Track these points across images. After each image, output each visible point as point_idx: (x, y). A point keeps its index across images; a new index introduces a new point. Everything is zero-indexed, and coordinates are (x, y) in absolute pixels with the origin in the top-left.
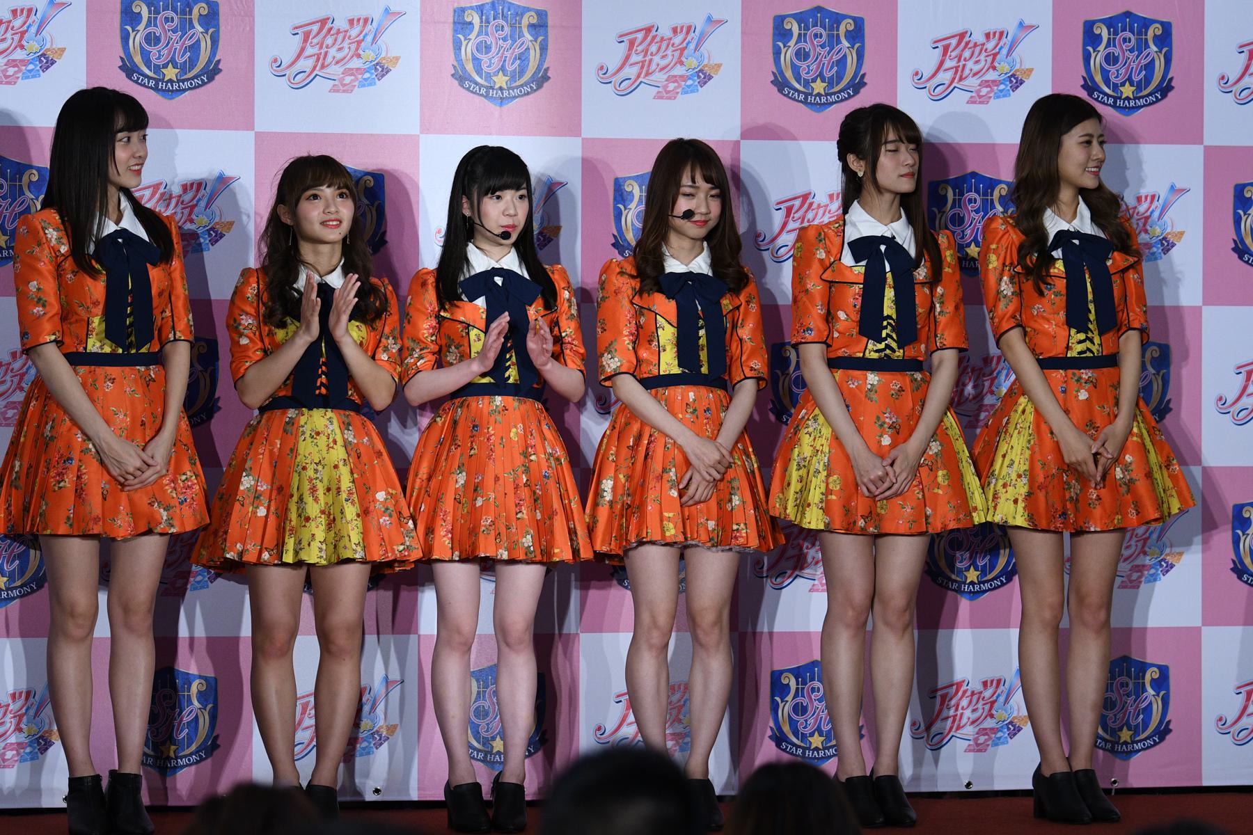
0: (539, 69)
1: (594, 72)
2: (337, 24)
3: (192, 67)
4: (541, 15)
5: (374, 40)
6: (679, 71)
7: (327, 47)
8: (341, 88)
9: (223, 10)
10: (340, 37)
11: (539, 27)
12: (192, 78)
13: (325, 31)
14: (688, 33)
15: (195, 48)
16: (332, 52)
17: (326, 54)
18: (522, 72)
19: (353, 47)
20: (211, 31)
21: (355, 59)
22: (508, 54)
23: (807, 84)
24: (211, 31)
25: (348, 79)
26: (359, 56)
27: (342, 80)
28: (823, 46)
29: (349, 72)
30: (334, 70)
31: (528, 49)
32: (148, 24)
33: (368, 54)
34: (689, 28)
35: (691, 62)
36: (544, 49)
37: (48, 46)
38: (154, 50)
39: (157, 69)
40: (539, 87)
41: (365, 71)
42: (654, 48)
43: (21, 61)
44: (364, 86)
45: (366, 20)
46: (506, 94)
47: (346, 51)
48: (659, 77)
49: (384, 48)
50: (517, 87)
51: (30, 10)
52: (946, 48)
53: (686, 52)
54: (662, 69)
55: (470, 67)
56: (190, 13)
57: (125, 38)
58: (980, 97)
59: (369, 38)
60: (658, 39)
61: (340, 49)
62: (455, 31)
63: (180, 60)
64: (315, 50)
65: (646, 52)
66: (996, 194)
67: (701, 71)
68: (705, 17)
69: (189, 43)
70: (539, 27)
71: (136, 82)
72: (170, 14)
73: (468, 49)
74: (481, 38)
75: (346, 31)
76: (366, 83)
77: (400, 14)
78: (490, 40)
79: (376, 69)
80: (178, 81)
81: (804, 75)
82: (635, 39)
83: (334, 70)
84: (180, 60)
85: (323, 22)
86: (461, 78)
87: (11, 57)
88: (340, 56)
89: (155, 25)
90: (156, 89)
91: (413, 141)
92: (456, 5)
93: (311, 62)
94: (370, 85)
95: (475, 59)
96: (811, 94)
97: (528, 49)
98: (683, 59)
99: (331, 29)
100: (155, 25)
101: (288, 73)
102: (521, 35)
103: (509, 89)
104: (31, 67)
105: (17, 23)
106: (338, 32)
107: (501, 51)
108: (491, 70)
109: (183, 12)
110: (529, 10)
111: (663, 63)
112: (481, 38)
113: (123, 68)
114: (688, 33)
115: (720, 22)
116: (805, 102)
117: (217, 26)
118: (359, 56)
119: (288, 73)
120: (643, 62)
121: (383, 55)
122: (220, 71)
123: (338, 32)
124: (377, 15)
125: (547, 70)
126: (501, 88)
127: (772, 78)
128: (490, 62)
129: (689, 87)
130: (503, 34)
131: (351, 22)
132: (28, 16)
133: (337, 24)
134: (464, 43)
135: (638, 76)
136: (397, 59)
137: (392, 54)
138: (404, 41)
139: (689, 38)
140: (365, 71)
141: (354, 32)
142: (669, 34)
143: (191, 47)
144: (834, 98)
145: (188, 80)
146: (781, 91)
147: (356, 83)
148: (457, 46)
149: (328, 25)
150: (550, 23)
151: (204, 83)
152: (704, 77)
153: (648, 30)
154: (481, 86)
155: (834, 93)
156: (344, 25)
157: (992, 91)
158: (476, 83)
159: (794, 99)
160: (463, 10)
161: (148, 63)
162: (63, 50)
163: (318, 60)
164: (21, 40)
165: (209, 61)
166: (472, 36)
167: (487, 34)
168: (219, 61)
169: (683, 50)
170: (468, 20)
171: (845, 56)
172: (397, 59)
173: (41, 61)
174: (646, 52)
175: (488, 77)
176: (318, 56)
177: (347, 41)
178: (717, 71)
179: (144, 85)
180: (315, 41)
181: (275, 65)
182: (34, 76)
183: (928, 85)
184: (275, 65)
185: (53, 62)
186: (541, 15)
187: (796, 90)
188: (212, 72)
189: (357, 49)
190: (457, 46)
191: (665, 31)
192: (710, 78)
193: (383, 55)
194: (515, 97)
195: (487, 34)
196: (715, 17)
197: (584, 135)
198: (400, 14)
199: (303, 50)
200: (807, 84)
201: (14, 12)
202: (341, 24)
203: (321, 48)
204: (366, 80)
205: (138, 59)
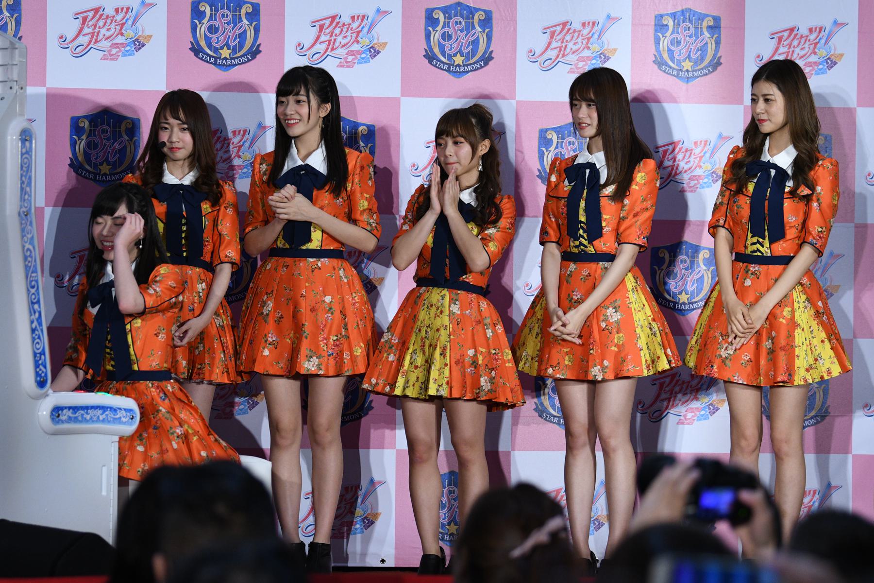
0: (714, 56)
2: (574, 26)
3: (473, 55)
4: (717, 19)
6: (813, 58)
7: (567, 42)
9: (494, 16)
12: (474, 63)
13: (565, 31)
14: (820, 32)
15: (475, 43)
16: (570, 45)
17: (566, 46)
18: (702, 59)
19: (585, 42)
20: (487, 30)
22: (692, 47)
24: (487, 30)
26: (588, 48)
27: (576, 65)
30: (572, 58)
31: (707, 43)
32: (444, 26)
33: (595, 47)
34: (821, 28)
35: (822, 52)
36: (718, 43)
37: (375, 41)
38: (447, 44)
39: (450, 57)
40: (715, 69)
41: (594, 58)
42: (795, 43)
43: (357, 51)
45: (594, 23)
46: (691, 75)
47: (580, 44)
49: (606, 43)
51: (363, 17)
52: (85, 20)
53: (818, 46)
55: (666, 56)
56: (473, 18)
59: (596, 36)
60: (798, 36)
61: (575, 43)
62: (656, 31)
63: (465, 51)
64: (559, 44)
65: (790, 45)
67: (829, 59)
68: (832, 21)
69: (472, 39)
70: (715, 28)
71: (435, 66)
72: (459, 19)
73: (665, 43)
77: (617, 19)
78: (680, 37)
79: (600, 58)
80: (464, 66)
82: (782, 36)
83: (572, 58)
84: (465, 51)
85: (564, 24)
86: (660, 63)
87: (350, 49)
88: (575, 48)
89: (449, 27)
90: (448, 71)
92: (657, 13)
93: (556, 52)
95: (669, 50)
97: (707, 43)
98: (816, 50)
99: (569, 29)
101: (539, 60)
102: (702, 34)
104: (364, 55)
105: (355, 25)
106: (575, 31)
107: (688, 44)
108: (681, 58)
110: (707, 16)
114: (820, 32)
115: (843, 25)
117: (491, 27)
118: (588, 48)
119: (539, 60)
121: (605, 47)
122: (493, 58)
123: (575, 31)
124: (601, 20)
126: (687, 71)
128: (680, 52)
129: (820, 70)
130: (690, 33)
131: (584, 24)
132: (362, 21)
133: (574, 26)
134: (662, 39)
136: (615, 50)
139: (821, 36)
140: (594, 58)
141: (585, 32)
143: (473, 42)
148: (657, 41)
149: (568, 27)
150: (722, 25)
151: (481, 67)
153: (792, 30)
154: (673, 69)
158: (671, 68)
160: (661, 16)
161: (443, 53)
163: (560, 50)
165: (485, 52)
166: (668, 34)
167: (678, 33)
168: (492, 52)
169: (816, 44)
170: (665, 22)
172: (615, 50)
173: (370, 52)
174: (790, 45)
175: (679, 63)
177: (581, 38)
178: (840, 59)
179: (440, 68)
180: (558, 38)
182: (366, 62)
185: (379, 52)
186: (717, 19)
188: (487, 59)
189: (587, 43)
190: (657, 41)
191: (803, 31)
192: (835, 63)
193: (605, 47)
194: (698, 77)
195: (678, 33)
196: (840, 21)
198: (617, 19)
199: (550, 44)
201: (353, 18)
202: (577, 26)
203: (562, 42)
205: (436, 50)
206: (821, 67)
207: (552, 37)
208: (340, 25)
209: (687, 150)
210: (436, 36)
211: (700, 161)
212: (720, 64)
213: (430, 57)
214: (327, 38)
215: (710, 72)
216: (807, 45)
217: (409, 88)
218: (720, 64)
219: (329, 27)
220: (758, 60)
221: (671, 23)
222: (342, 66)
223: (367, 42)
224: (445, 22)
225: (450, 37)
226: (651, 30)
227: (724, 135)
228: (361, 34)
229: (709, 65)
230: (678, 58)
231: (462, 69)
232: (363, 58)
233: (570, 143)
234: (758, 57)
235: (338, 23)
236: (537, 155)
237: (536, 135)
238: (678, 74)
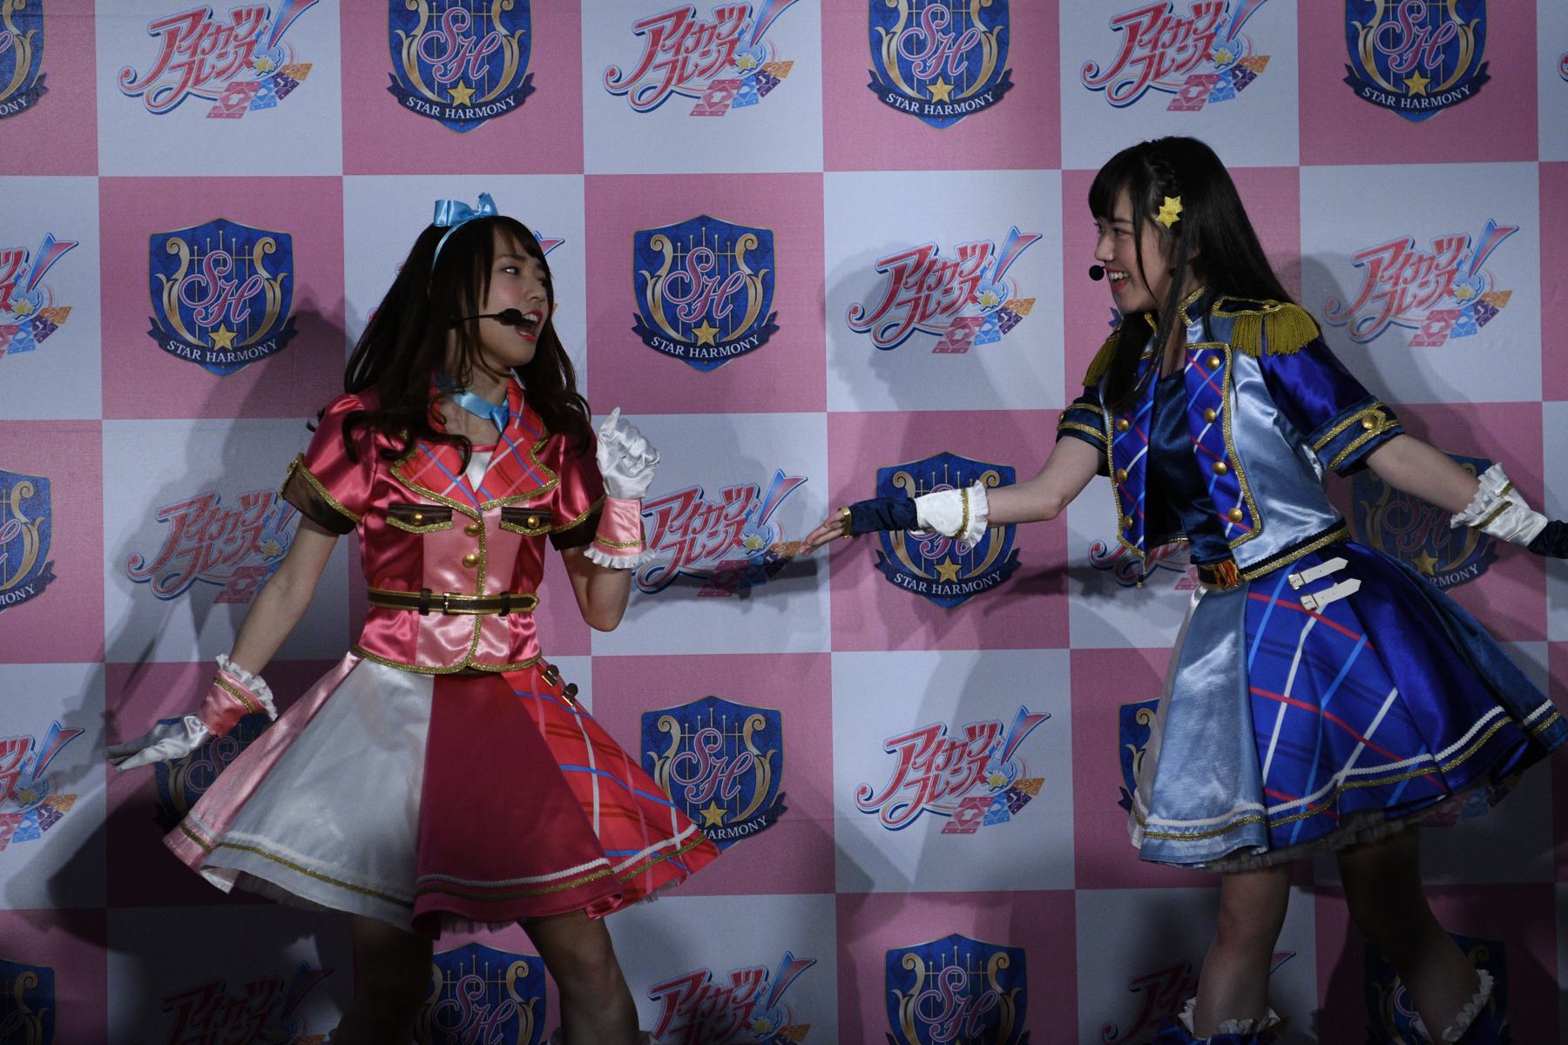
0: (996, 73)
1: (1078, 78)
5: (755, 39)
6: (1205, 68)
8: (707, 109)
10: (705, 36)
11: (996, 14)
12: (493, 102)
13: (683, 28)
15: (496, 58)
17: (685, 60)
18: (972, 76)
19: (724, 49)
21: (727, 67)
23: (1398, 80)
25: (717, 96)
27: (710, 96)
28: (1422, 25)
29: (719, 85)
30: (699, 84)
31: (980, 44)
33: (746, 59)
34: (1219, 6)
35: (1223, 54)
36: (1003, 43)
38: (437, 63)
39: (442, 90)
40: (998, 97)
44: (740, 105)
45: (742, 10)
49: (769, 50)
50: (964, 100)
55: (895, 74)
57: (396, 46)
60: (1172, 23)
61: (704, 54)
62: (872, 24)
64: (669, 56)
67: (1238, 67)
71: (413, 109)
73: (893, 46)
74: (911, 31)
75: (715, 27)
76: (748, 101)
78: (922, 33)
80: (473, 106)
82: (1138, 25)
83: (699, 84)
85: (680, 15)
86: (882, 88)
91: (812, 183)
94: (749, 103)
99: (691, 25)
100: (439, 28)
102: (970, 24)
103: (953, 102)
104: (262, 92)
106: (702, 28)
107: (943, 49)
109: (479, 9)
111: (1181, 58)
112: (911, 31)
113: (394, 89)
116: (1396, 107)
118: (732, 62)
120: (1151, 58)
121: (768, 59)
122: (533, 89)
123: (702, 28)
125: (1009, 73)
127: (1346, 74)
134: (886, 40)
135: (1145, 78)
136: (789, 64)
137: (782, 57)
138: (797, 38)
140: (742, 83)
141: (725, 29)
142: (1188, 14)
145: (486, 104)
146: (1359, 92)
147: (729, 102)
149: (689, 19)
151: (510, 109)
155: (1441, 93)
156: (711, 19)
158: (905, 96)
159: (1380, 104)
161: (429, 84)
162: (308, 67)
164: (249, 52)
167: (919, 25)
171: (1456, 38)
172: (789, 64)
176: (674, 63)
177: (715, 42)
179: (424, 114)
180: (669, 43)
181: (611, 80)
182: (267, 105)
184: (611, 80)
185: (294, 85)
187: (1382, 90)
188: (521, 92)
189: (730, 52)
190: (876, 43)
193: (768, 59)
194: (962, 115)
195: (919, 25)
197: (1066, 165)
199: (650, 56)
201: (238, 16)
202: (706, 17)
203: (677, 52)
204: (744, 96)
205: (415, 77)
207: (655, 43)
208: (212, 30)
210: (413, 48)
212: (1012, 85)
213: (402, 91)
214: (185, 58)
215: (988, 104)
216: (1190, 41)
217: (364, 154)
218: (1012, 85)
219: (190, 32)
221: (903, 8)
222: (219, 116)
223: (271, 63)
224: (430, 19)
225: (442, 50)
226: (863, 18)
227: (1024, 230)
228: (256, 48)
229: (986, 89)
231: (470, 114)
232: (261, 98)
233: (700, 259)
234: (1090, 68)
235: (207, 27)
236: (632, 286)
237: (630, 245)
238: (922, 109)
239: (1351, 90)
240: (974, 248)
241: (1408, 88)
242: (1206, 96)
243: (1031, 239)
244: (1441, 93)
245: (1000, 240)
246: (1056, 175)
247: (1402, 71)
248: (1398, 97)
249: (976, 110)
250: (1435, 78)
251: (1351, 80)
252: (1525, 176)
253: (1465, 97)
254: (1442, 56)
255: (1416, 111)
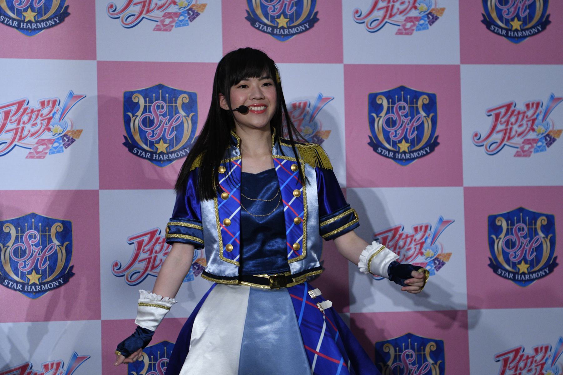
0: (60, 7)
6: (173, 9)
23: (273, 19)
40: (62, 20)
48: (158, 14)
50: (43, 21)
54: (159, 8)
58: (406, 29)
66: (420, 103)
67: (191, 9)
81: (270, 13)
96: (277, 28)
116: (272, 33)
125: (67, 7)
127: (246, 15)
129: (181, 21)
135: (141, 13)
144: (294, 30)
146: (253, 24)
152: (193, 14)
155: (295, 27)
157: (414, 25)
159: (264, 31)
178: (203, 10)
183: (366, 20)
192: (198, 14)
194: (41, 29)
200: (273, 19)
206: (182, 18)
209: (32, 111)
211: (48, 123)
212: (69, 14)
215: (56, 24)
218: (69, 14)
220: (111, 10)
227: (76, 93)
229: (55, 15)
230: (19, 7)
234: (111, 6)
238: (19, 25)
239: (248, 23)
240: (49, 102)
241: (278, 23)
242: (174, 24)
243: (80, 97)
244: (295, 27)
245: (63, 98)
246: (94, 63)
247: (275, 14)
248: (273, 28)
249: (49, 27)
250: (291, 19)
251: (249, 18)
252: (337, 70)
253: (307, 29)
254: (295, 8)
255: (283, 35)
